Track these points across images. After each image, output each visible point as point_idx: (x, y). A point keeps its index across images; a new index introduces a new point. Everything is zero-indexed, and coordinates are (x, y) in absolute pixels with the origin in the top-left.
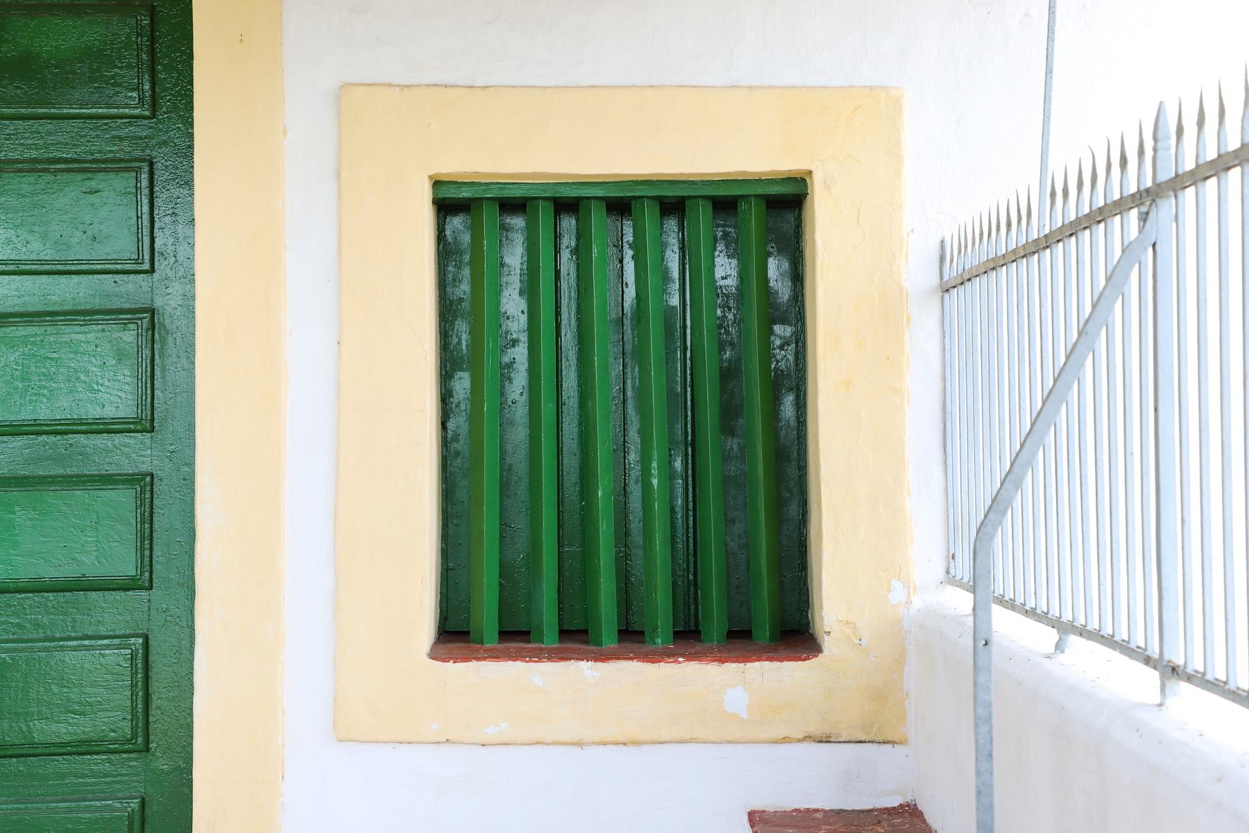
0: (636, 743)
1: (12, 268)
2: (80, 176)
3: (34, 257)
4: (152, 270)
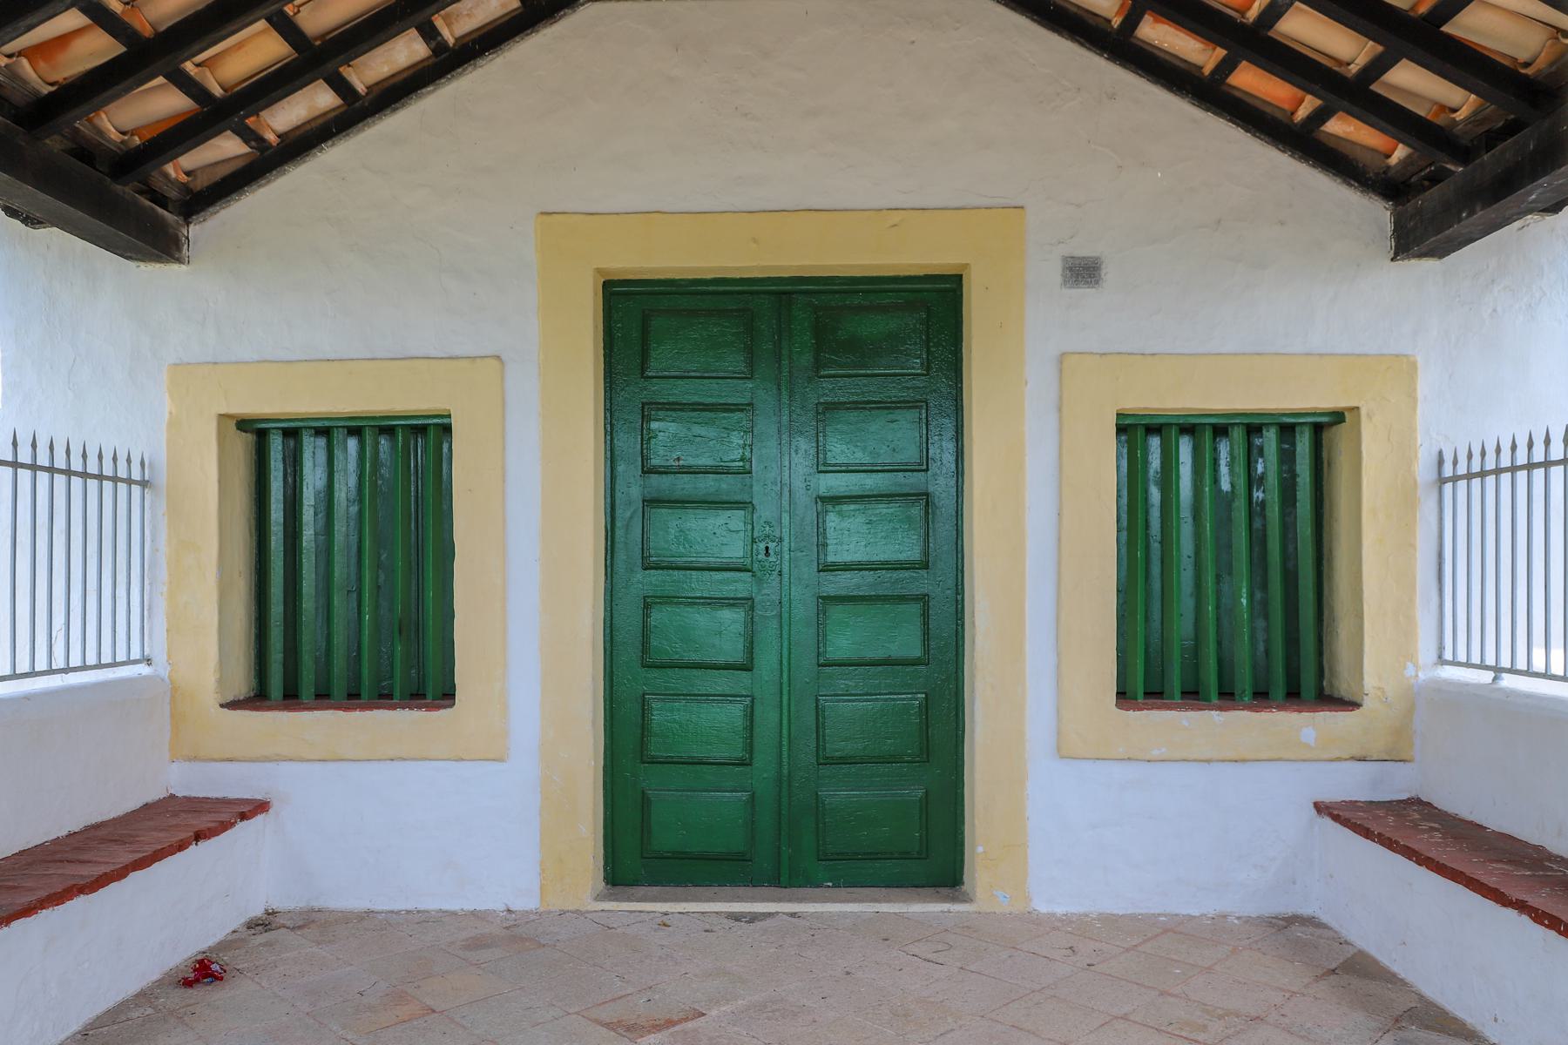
0: (1244, 761)
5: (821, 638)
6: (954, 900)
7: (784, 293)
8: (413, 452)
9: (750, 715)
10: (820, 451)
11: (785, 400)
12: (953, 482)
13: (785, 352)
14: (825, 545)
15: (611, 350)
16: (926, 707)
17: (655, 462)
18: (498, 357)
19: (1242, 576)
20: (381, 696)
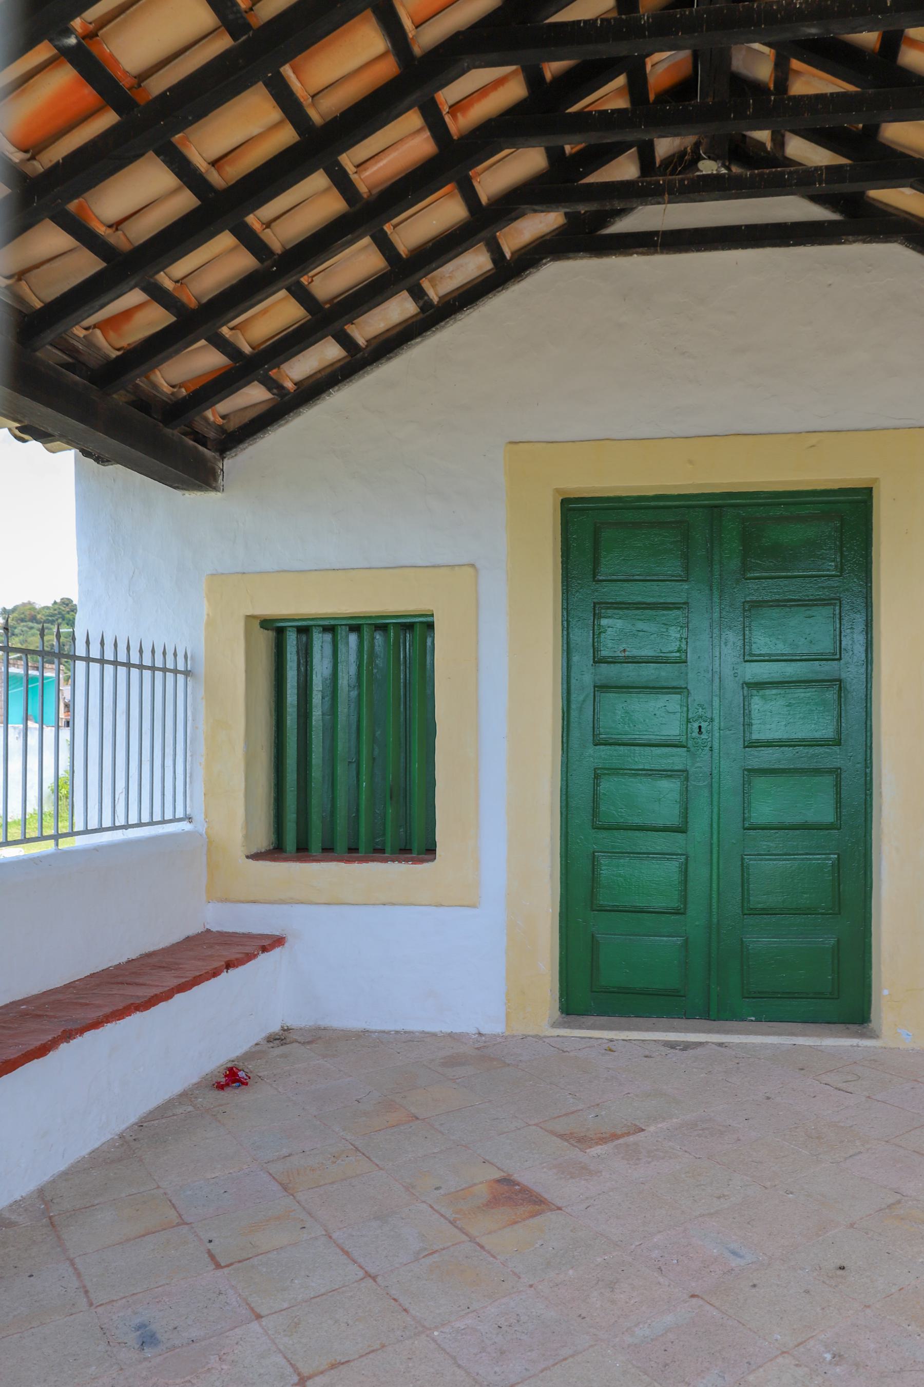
1: (767, 658)
2: (804, 608)
3: (779, 652)
4: (840, 659)
5: (746, 805)
6: (863, 1036)
7: (716, 507)
8: (402, 646)
9: (685, 871)
10: (746, 642)
11: (716, 599)
12: (863, 670)
13: (716, 558)
14: (750, 725)
15: (568, 558)
16: (838, 866)
17: (604, 653)
18: (473, 566)
20: (376, 851)
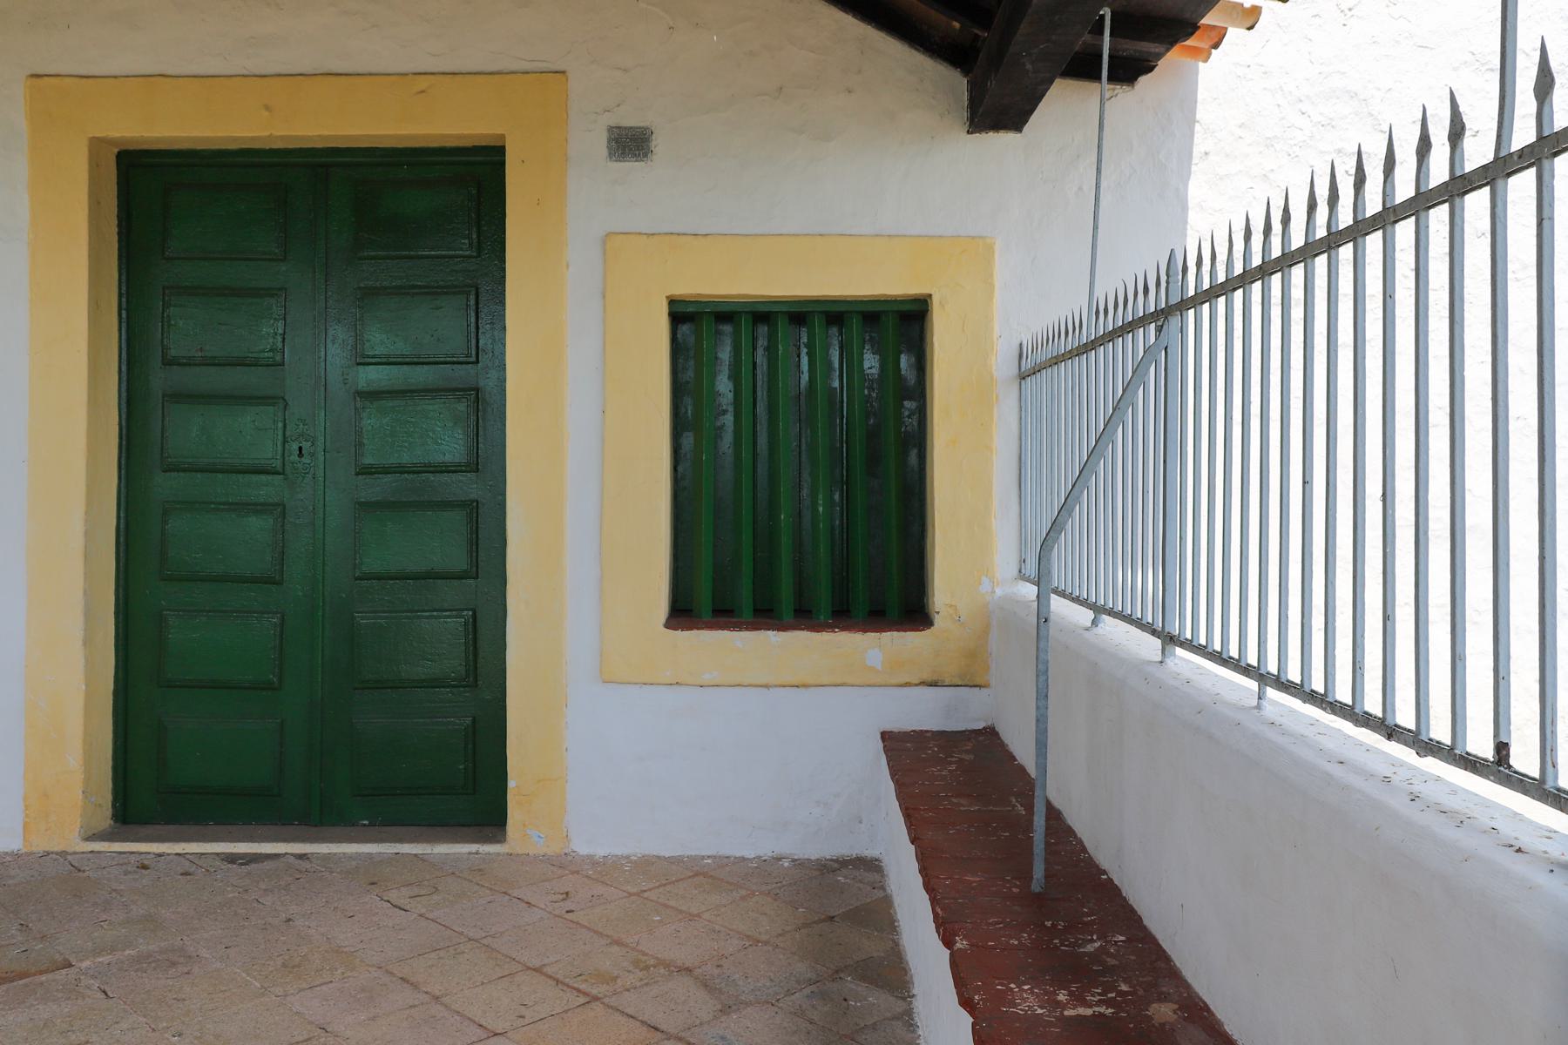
0: (805, 686)
17: (173, 353)
19: (809, 475)
